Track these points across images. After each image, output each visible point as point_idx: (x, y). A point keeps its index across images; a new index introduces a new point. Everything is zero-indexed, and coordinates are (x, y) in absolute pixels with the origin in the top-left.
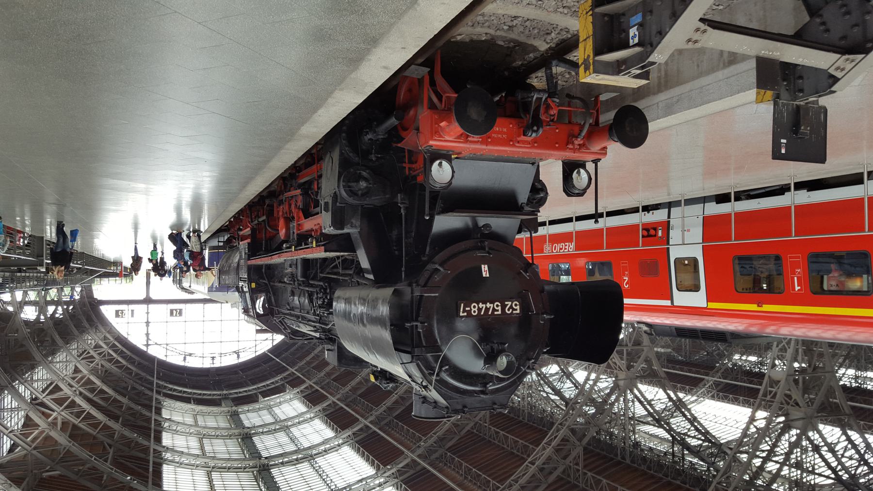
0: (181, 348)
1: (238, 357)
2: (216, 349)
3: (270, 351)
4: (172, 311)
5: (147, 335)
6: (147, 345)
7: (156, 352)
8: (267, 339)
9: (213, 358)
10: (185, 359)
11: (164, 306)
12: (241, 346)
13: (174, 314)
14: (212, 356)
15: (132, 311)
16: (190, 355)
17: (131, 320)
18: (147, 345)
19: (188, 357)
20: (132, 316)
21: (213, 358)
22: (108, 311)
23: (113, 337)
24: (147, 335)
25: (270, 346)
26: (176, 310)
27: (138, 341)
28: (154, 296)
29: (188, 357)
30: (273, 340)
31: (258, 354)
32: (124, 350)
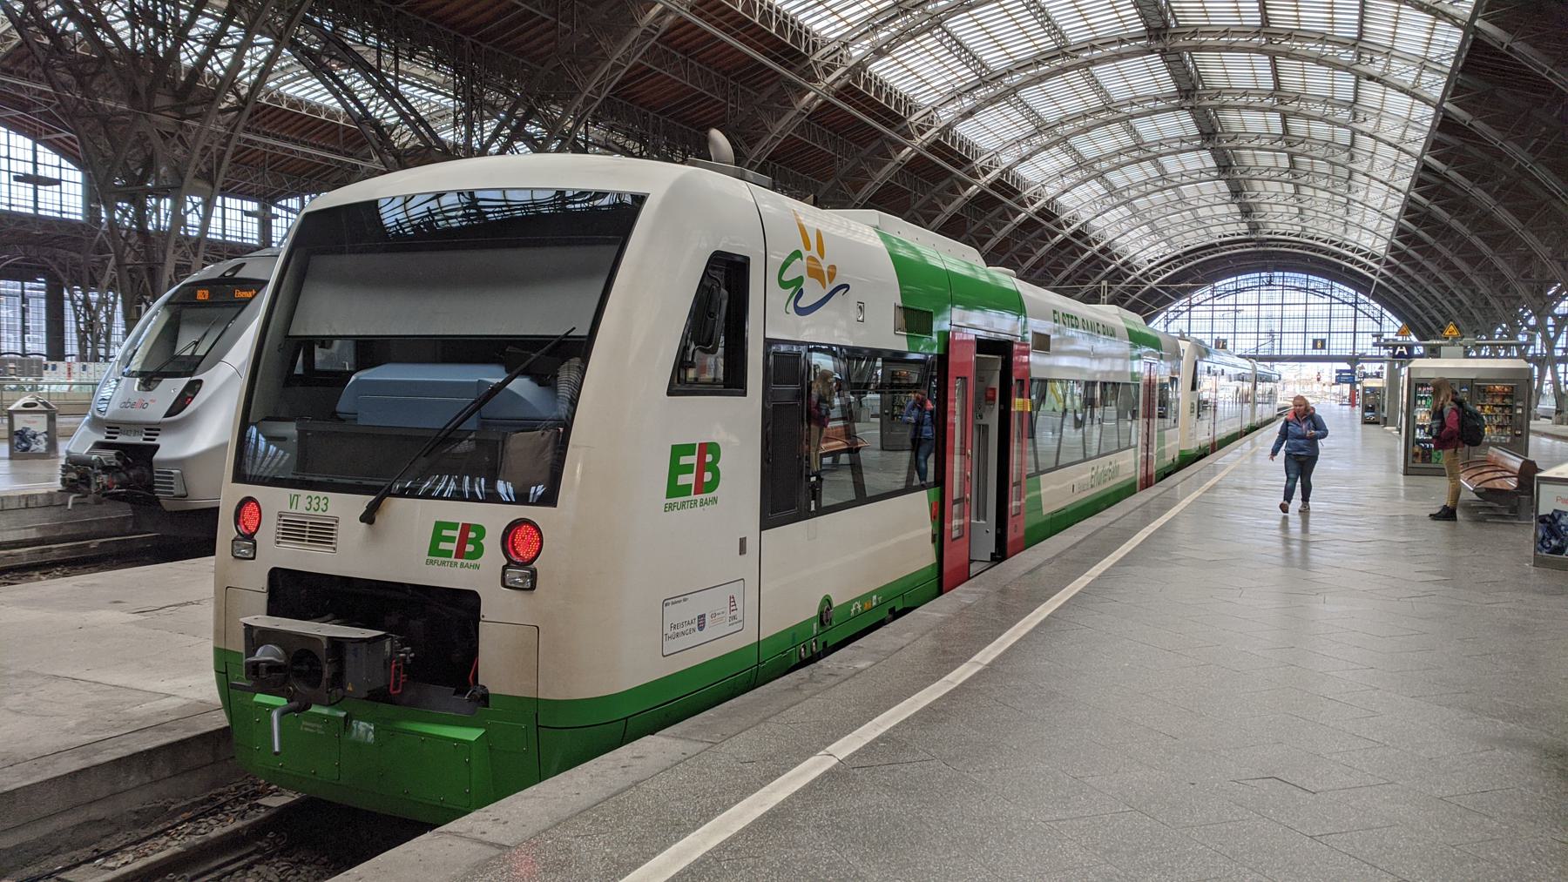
0: (1312, 298)
2: (1265, 296)
4: (1323, 347)
11: (1333, 353)
12: (1230, 299)
14: (1271, 287)
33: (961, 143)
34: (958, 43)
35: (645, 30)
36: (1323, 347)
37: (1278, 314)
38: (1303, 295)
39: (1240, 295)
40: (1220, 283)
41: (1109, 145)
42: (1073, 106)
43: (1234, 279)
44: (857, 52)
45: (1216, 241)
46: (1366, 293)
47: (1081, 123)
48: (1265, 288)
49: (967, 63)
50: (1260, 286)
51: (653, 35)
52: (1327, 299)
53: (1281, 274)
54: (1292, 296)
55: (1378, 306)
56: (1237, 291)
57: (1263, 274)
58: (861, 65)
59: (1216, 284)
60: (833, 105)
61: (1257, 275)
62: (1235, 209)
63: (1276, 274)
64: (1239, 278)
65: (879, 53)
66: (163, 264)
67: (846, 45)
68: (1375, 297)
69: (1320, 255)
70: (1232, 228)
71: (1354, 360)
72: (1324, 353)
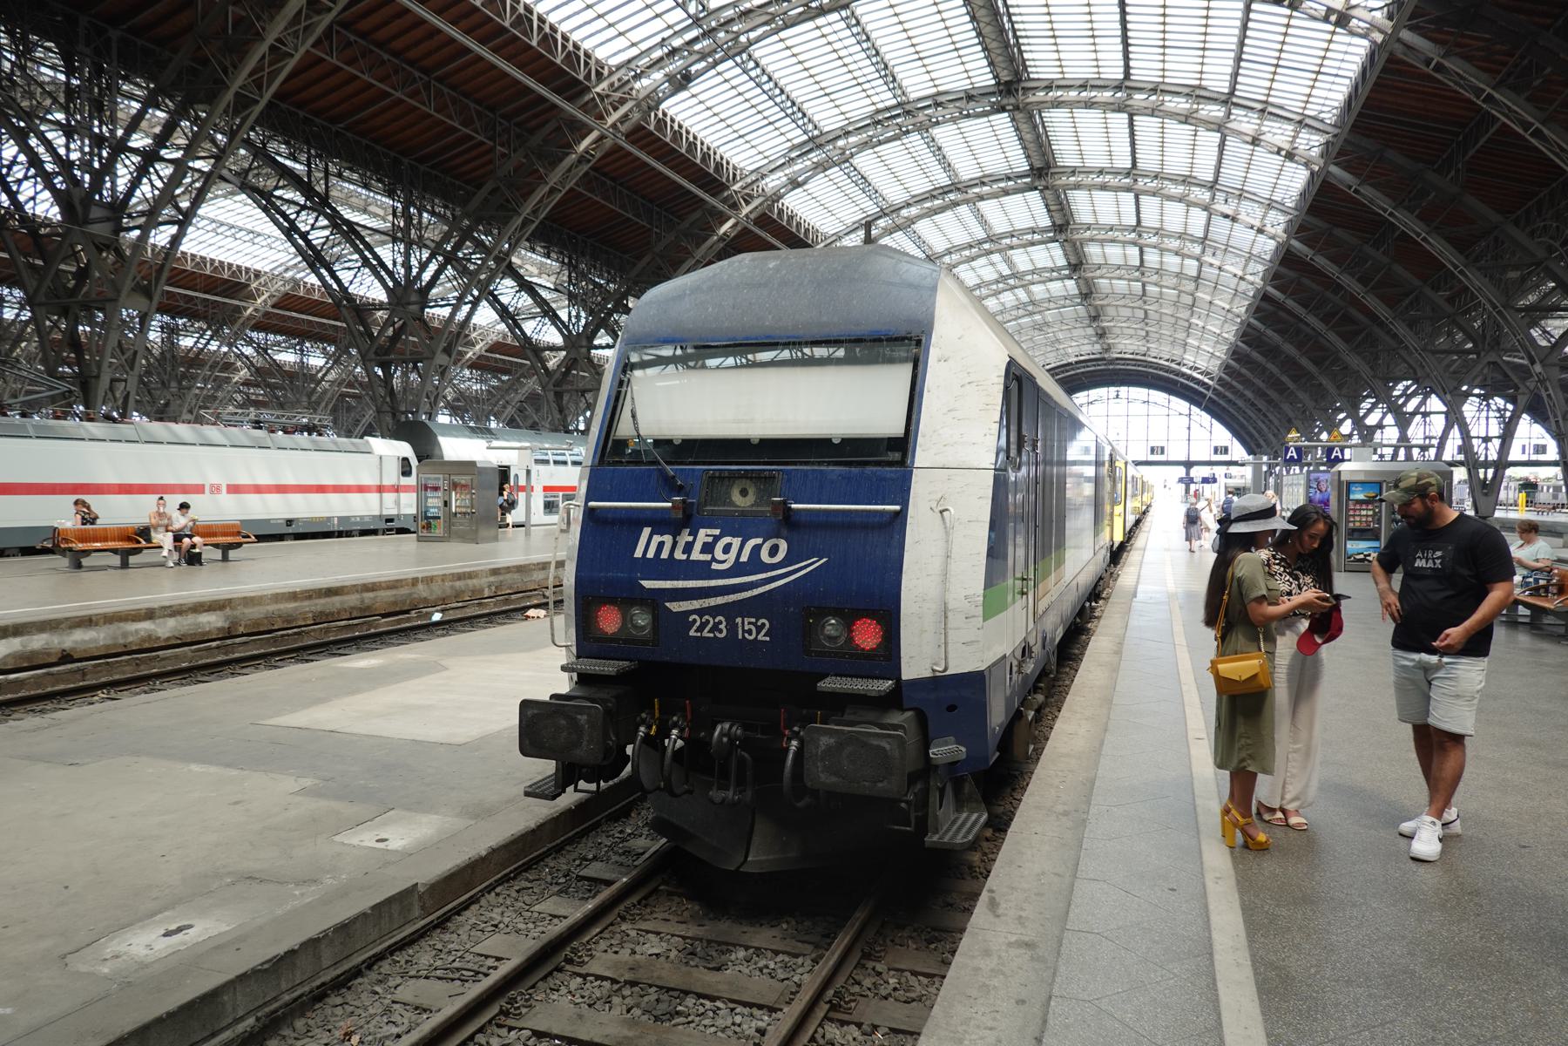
0: (1153, 409)
9: (1117, 396)
21: (1117, 396)
33: (807, 230)
34: (863, 177)
35: (582, 156)
41: (989, 274)
42: (961, 238)
43: (1085, 393)
44: (773, 182)
45: (1073, 360)
46: (1198, 405)
47: (967, 253)
49: (847, 174)
51: (589, 161)
52: (1165, 411)
55: (1209, 417)
58: (777, 197)
60: (751, 232)
62: (1090, 331)
65: (795, 184)
66: (97, 377)
67: (763, 176)
68: (1207, 410)
69: (1161, 373)
70: (1087, 349)
71: (1189, 465)
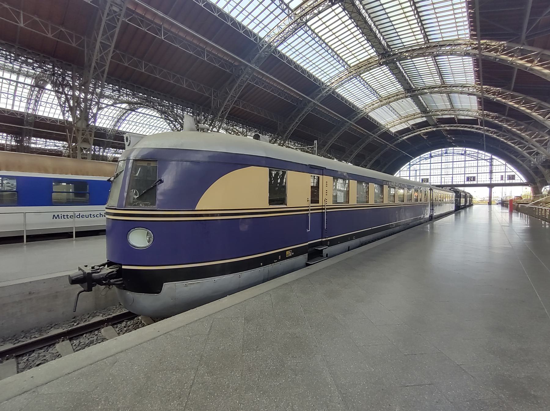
0: (468, 158)
1: (431, 155)
3: (412, 159)
5: (491, 165)
6: (492, 159)
7: (484, 154)
8: (413, 165)
9: (446, 153)
10: (465, 152)
11: (479, 183)
13: (472, 178)
14: (447, 155)
15: (502, 179)
16: (462, 154)
17: (503, 174)
18: (492, 159)
19: (463, 152)
20: (502, 177)
22: (520, 178)
23: (518, 163)
24: (491, 165)
25: (411, 161)
26: (471, 181)
27: (498, 162)
28: (487, 189)
29: (463, 152)
30: (410, 165)
31: (419, 157)
32: (509, 154)
36: (474, 180)
37: (451, 166)
38: (463, 157)
39: (432, 159)
40: (423, 155)
48: (444, 155)
50: (442, 154)
53: (452, 148)
54: (457, 158)
56: (431, 157)
57: (443, 149)
59: (421, 156)
61: (440, 150)
63: (449, 149)
64: (432, 152)
72: (475, 182)
